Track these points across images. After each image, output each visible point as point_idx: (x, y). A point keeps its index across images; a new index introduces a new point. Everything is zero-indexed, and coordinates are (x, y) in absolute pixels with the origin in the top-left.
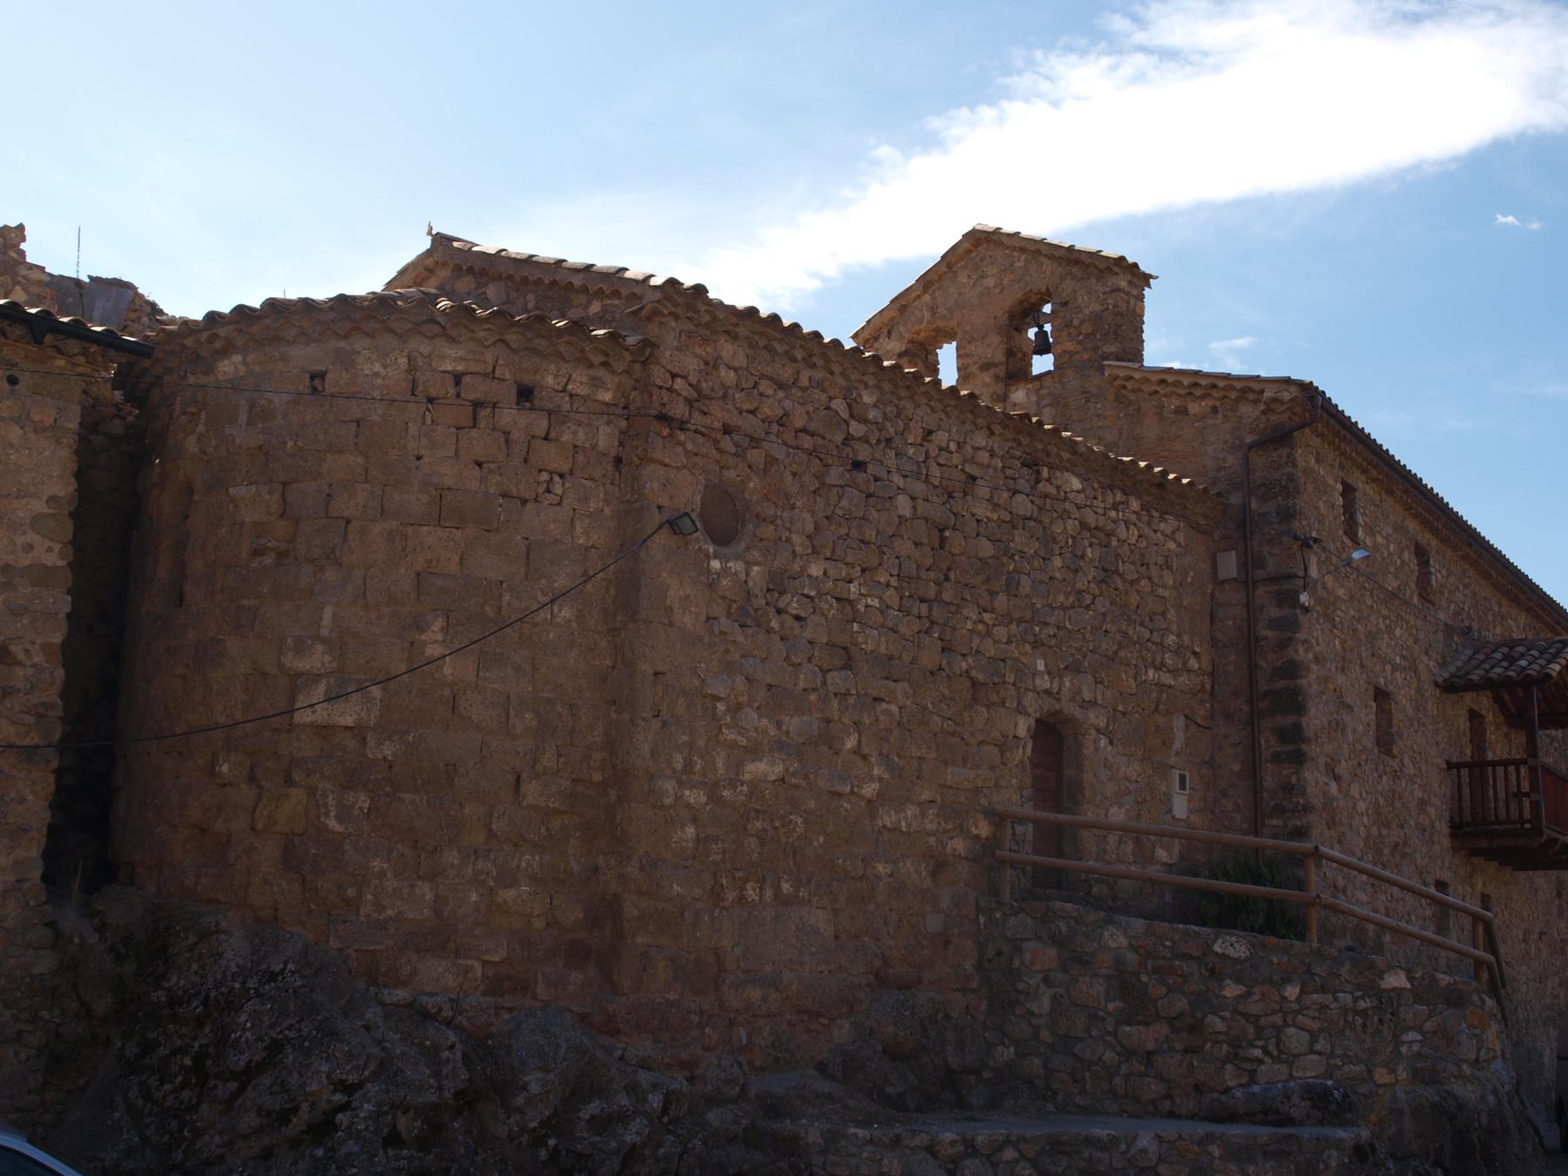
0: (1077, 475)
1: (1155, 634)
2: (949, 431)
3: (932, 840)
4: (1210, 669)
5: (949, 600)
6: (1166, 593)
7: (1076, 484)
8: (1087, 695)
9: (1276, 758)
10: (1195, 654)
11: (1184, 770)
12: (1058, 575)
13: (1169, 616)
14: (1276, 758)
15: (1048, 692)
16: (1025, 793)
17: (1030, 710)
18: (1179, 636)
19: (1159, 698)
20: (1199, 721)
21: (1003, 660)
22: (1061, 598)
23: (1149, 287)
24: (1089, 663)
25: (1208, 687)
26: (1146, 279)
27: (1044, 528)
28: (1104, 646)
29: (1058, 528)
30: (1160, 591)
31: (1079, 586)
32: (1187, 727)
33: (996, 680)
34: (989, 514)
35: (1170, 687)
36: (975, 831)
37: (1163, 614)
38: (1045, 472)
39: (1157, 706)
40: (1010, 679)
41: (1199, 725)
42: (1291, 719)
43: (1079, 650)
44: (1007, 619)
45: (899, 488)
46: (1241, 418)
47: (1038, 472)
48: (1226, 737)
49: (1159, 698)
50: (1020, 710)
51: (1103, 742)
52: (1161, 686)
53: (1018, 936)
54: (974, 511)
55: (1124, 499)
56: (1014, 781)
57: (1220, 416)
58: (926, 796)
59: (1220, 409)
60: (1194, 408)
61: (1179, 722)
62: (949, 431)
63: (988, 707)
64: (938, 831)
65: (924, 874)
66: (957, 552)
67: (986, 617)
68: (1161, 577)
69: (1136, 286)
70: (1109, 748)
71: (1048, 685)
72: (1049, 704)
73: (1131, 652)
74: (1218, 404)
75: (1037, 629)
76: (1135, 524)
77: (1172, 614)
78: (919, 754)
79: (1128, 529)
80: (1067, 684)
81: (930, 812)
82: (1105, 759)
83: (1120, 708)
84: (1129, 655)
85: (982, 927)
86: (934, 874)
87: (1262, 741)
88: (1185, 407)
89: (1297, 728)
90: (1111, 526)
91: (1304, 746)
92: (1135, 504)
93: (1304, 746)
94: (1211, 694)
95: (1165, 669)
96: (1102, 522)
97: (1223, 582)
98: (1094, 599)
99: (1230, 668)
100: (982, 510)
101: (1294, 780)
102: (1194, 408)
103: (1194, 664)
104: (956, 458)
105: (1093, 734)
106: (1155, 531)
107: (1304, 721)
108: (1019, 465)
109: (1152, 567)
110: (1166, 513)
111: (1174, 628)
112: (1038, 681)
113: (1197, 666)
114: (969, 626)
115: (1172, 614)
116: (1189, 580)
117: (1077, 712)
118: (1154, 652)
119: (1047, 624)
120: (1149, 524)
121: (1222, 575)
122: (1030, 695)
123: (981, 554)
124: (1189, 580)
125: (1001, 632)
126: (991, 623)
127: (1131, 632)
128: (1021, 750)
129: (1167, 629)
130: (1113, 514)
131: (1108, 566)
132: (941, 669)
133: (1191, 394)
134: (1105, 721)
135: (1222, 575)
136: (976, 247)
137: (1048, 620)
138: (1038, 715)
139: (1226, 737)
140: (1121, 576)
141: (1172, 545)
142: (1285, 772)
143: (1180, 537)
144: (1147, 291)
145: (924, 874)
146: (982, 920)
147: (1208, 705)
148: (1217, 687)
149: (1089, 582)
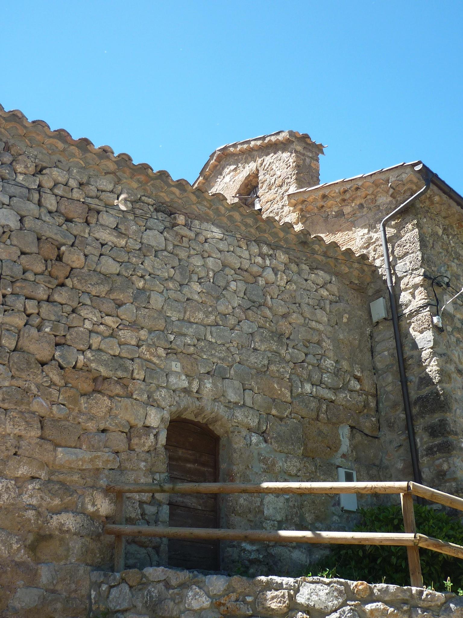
0: (218, 226)
1: (310, 357)
2: (69, 171)
3: (30, 514)
4: (373, 391)
5: (64, 302)
6: (321, 327)
7: (217, 233)
8: (232, 397)
9: (430, 451)
10: (358, 379)
11: (352, 470)
12: (196, 297)
13: (324, 344)
14: (430, 451)
15: (186, 391)
16: (157, 476)
17: (163, 404)
18: (337, 362)
19: (319, 410)
20: (367, 431)
21: (132, 360)
22: (201, 315)
23: (323, 153)
24: (235, 372)
25: (373, 405)
26: (319, 149)
27: (180, 260)
28: (253, 359)
29: (197, 261)
30: (313, 324)
31: (221, 308)
32: (352, 437)
33: (120, 374)
34: (115, 240)
35: (332, 402)
36: (90, 509)
37: (319, 343)
38: (181, 219)
39: (318, 416)
40: (139, 375)
41: (367, 435)
42: (436, 418)
43: (222, 359)
44: (134, 326)
45: (3, 204)
46: (379, 206)
47: (175, 218)
48: (391, 442)
49: (319, 410)
50: (151, 402)
51: (255, 439)
52: (321, 400)
53: (118, 608)
54: (97, 235)
55: (271, 252)
56: (143, 464)
57: (365, 209)
58: (23, 471)
59: (365, 205)
60: (347, 210)
61: (344, 432)
62: (69, 171)
63: (110, 397)
64: (40, 506)
65: (15, 547)
66: (78, 266)
67: (109, 320)
68: (315, 314)
69: (310, 151)
70: (263, 445)
71: (186, 384)
72: (185, 401)
73: (283, 368)
74: (363, 201)
75: (172, 337)
76: (284, 272)
77: (327, 344)
78: (16, 431)
79: (276, 274)
80: (209, 386)
81: (30, 487)
82: (259, 454)
83: (274, 412)
84: (282, 370)
85: (93, 601)
86: (33, 548)
87: (418, 440)
88: (342, 211)
89: (443, 423)
90: (255, 269)
91: (451, 438)
92: (282, 257)
93: (451, 438)
94: (377, 411)
95: (324, 386)
96: (246, 265)
97: (378, 323)
98: (239, 322)
99: (389, 388)
100: (105, 236)
101: (445, 467)
102: (347, 210)
103: (355, 385)
104: (76, 194)
105: (244, 432)
106: (306, 280)
107: (449, 417)
108: (152, 210)
109: (303, 306)
110: (316, 269)
111: (331, 354)
112: (173, 379)
113: (358, 387)
114: (88, 325)
115: (327, 344)
116: (345, 320)
117: (222, 411)
118: (310, 371)
119: (185, 335)
120: (299, 274)
121: (375, 319)
122: (164, 392)
123: (103, 270)
124: (345, 320)
125: (126, 335)
126: (115, 326)
127: (283, 352)
128: (152, 437)
129: (323, 355)
130: (259, 260)
131: (254, 298)
132: (53, 358)
133: (344, 200)
134: (257, 420)
135: (375, 319)
136: (219, 162)
137: (184, 330)
138: (174, 409)
139: (391, 442)
140: (270, 309)
141: (325, 293)
142: (437, 462)
143: (334, 289)
144: (320, 156)
145: (15, 547)
146: (93, 593)
147: (374, 419)
148: (381, 405)
149: (233, 308)
